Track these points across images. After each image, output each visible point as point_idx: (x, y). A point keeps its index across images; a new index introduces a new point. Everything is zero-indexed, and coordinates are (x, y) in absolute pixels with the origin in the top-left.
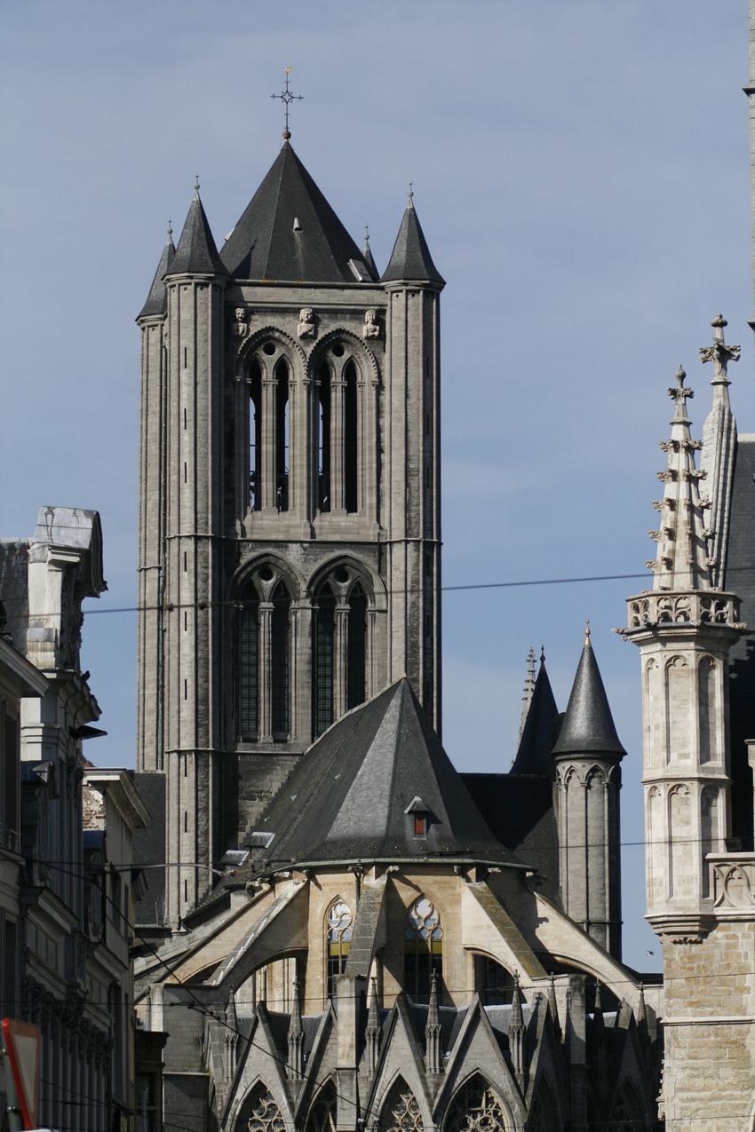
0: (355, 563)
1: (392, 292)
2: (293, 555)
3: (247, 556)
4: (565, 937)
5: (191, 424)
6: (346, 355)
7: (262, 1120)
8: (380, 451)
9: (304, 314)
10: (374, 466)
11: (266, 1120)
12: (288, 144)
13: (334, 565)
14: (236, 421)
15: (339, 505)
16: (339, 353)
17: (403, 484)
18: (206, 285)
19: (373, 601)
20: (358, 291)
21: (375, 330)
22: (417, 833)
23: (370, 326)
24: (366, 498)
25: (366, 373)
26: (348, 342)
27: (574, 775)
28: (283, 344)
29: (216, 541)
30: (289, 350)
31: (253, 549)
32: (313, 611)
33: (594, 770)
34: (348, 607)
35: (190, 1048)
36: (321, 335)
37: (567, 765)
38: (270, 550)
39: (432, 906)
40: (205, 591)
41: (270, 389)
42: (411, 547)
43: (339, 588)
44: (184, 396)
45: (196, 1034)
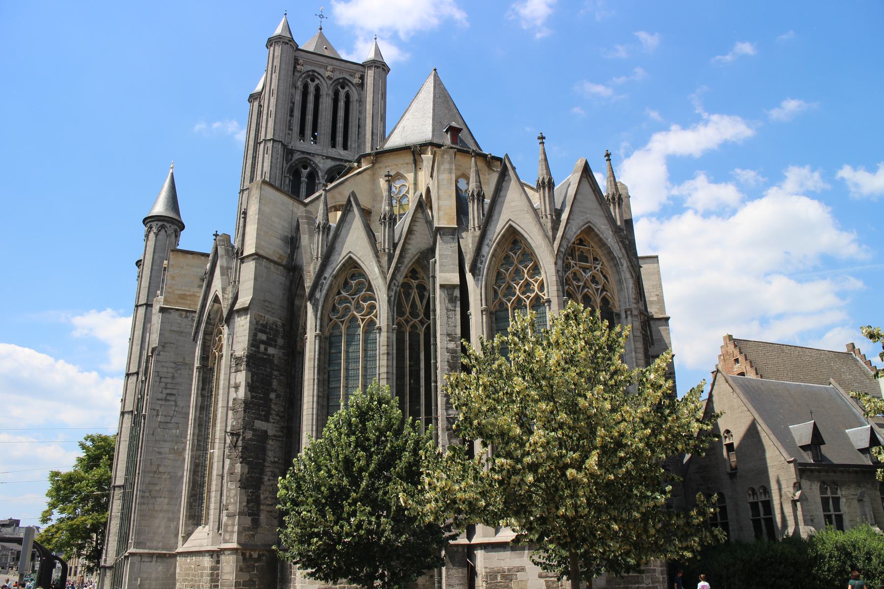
2: (317, 160)
3: (297, 156)
6: (347, 89)
7: (350, 297)
8: (359, 126)
9: (329, 68)
11: (353, 297)
12: (321, 32)
14: (296, 102)
15: (340, 146)
16: (343, 88)
18: (288, 43)
23: (357, 79)
24: (352, 143)
28: (318, 79)
29: (284, 146)
30: (321, 82)
31: (299, 155)
35: (279, 242)
36: (335, 78)
40: (276, 164)
41: (312, 95)
45: (286, 234)
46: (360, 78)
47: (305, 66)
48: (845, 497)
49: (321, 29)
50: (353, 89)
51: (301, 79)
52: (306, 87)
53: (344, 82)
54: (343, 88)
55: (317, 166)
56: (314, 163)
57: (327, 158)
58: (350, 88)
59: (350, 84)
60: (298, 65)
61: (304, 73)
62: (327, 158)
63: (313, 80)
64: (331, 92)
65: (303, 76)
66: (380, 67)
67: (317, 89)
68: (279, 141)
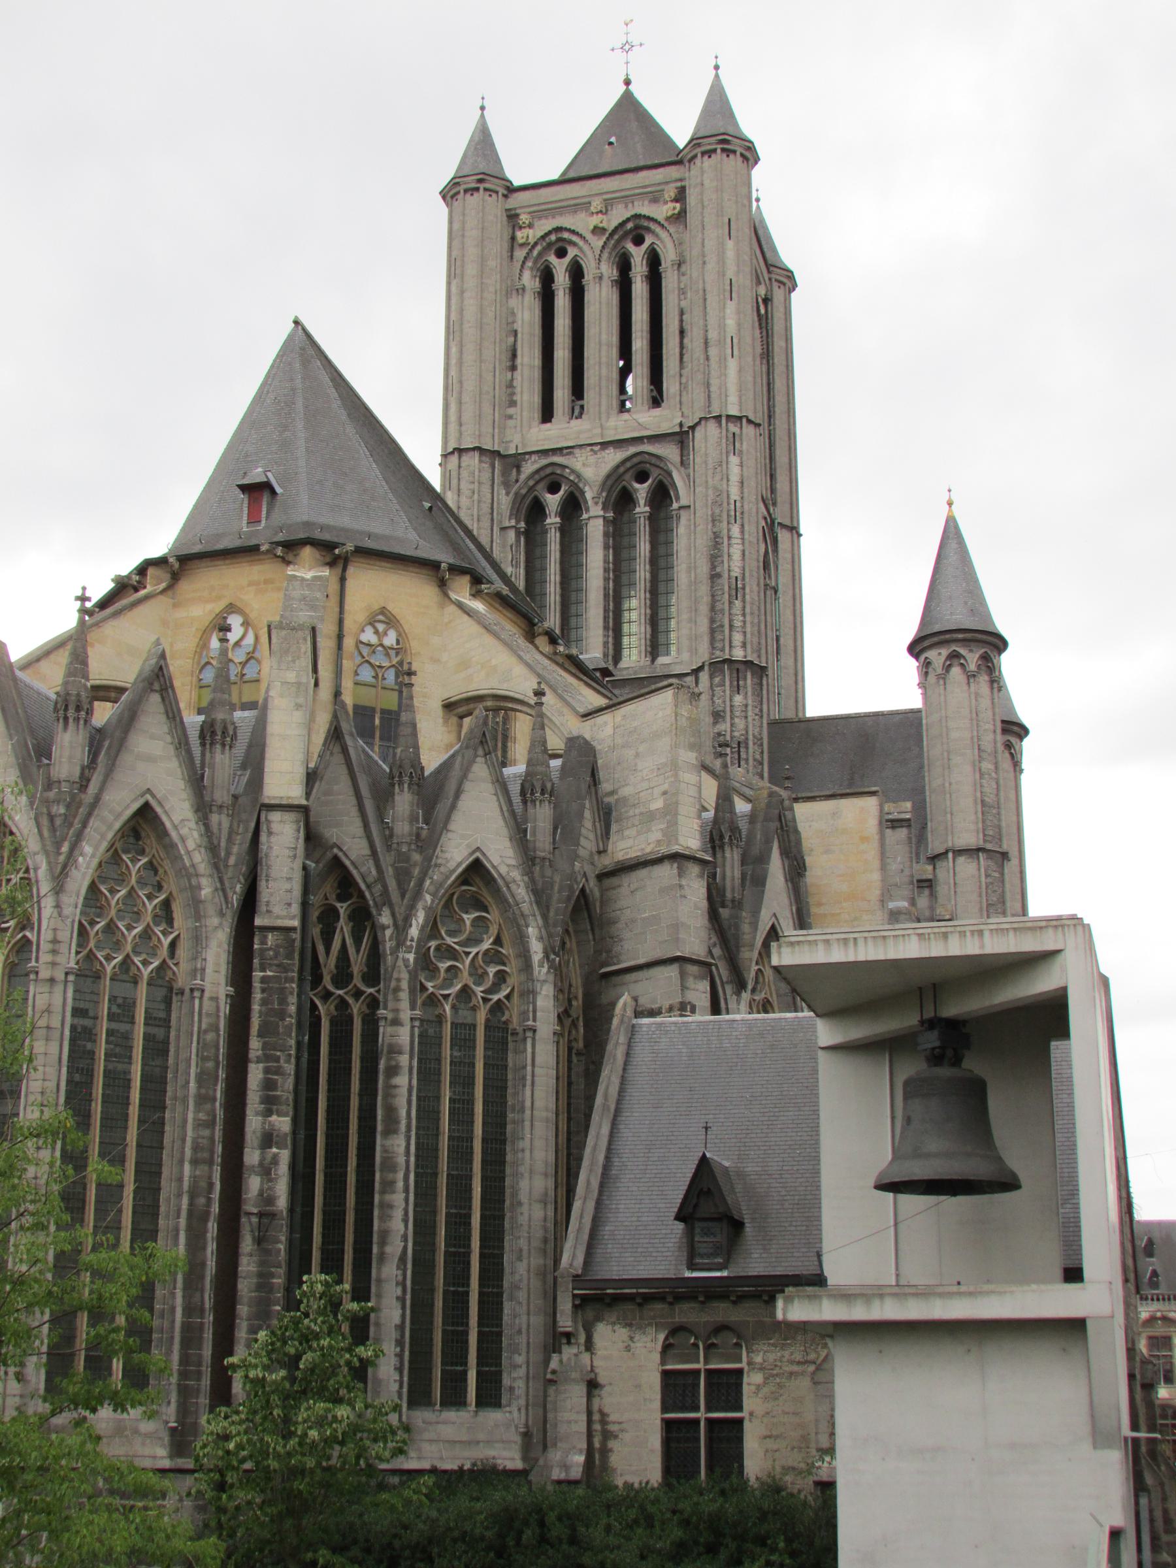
0: (654, 461)
1: (690, 161)
3: (529, 468)
4: (494, 662)
5: (457, 334)
8: (682, 332)
10: (677, 350)
13: (628, 465)
14: (519, 330)
16: (639, 241)
17: (702, 357)
18: (477, 189)
19: (678, 499)
20: (654, 172)
21: (674, 209)
22: (254, 519)
23: (671, 205)
24: (670, 385)
25: (668, 255)
26: (648, 229)
27: (930, 670)
28: (574, 244)
30: (581, 249)
32: (604, 518)
33: (955, 656)
34: (647, 509)
37: (922, 658)
38: (557, 459)
39: (246, 624)
42: (712, 426)
43: (636, 490)
44: (453, 308)
46: (676, 200)
47: (536, 224)
48: (761, 1369)
49: (627, 83)
50: (663, 234)
51: (529, 264)
52: (547, 277)
53: (637, 227)
54: (639, 241)
55: (579, 476)
56: (573, 471)
57: (605, 445)
58: (657, 236)
59: (652, 226)
60: (521, 228)
61: (534, 246)
62: (605, 445)
63: (561, 253)
64: (609, 271)
65: (535, 253)
66: (715, 151)
67: (576, 272)
68: (474, 449)
